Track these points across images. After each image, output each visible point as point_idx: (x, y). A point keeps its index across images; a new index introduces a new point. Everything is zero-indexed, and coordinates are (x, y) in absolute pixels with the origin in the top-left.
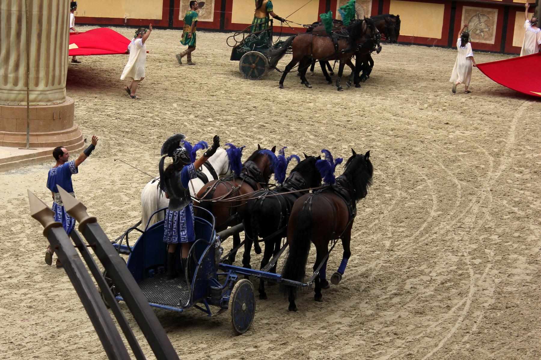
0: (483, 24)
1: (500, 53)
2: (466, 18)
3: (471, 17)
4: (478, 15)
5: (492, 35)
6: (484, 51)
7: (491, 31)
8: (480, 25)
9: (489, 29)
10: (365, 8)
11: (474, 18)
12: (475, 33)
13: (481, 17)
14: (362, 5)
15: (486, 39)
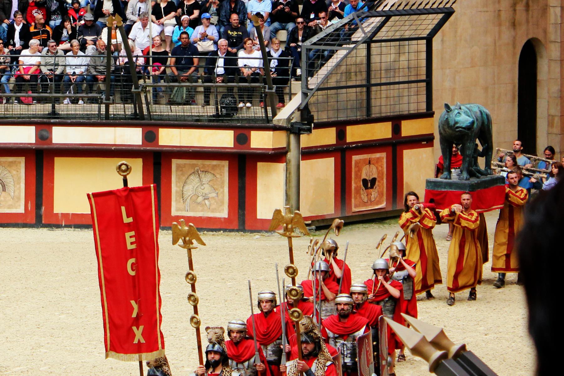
0: (206, 186)
1: (238, 231)
2: (179, 178)
3: (186, 176)
4: (198, 172)
5: (223, 203)
6: (212, 230)
7: (220, 197)
8: (202, 187)
9: (217, 193)
10: (14, 172)
11: (192, 177)
12: (195, 201)
13: (202, 175)
14: (9, 169)
15: (213, 211)
